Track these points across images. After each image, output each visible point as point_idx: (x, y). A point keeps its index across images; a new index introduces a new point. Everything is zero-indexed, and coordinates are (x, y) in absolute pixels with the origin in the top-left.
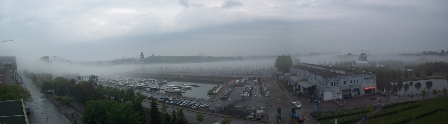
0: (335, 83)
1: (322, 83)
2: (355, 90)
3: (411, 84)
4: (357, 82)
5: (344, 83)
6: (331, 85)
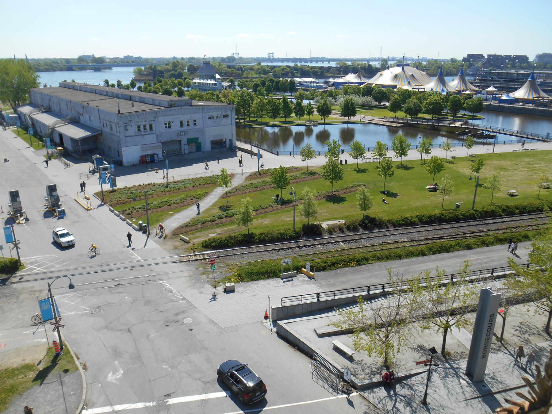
0: (145, 126)
2: (190, 141)
3: (309, 131)
4: (195, 124)
5: (166, 127)
6: (136, 132)
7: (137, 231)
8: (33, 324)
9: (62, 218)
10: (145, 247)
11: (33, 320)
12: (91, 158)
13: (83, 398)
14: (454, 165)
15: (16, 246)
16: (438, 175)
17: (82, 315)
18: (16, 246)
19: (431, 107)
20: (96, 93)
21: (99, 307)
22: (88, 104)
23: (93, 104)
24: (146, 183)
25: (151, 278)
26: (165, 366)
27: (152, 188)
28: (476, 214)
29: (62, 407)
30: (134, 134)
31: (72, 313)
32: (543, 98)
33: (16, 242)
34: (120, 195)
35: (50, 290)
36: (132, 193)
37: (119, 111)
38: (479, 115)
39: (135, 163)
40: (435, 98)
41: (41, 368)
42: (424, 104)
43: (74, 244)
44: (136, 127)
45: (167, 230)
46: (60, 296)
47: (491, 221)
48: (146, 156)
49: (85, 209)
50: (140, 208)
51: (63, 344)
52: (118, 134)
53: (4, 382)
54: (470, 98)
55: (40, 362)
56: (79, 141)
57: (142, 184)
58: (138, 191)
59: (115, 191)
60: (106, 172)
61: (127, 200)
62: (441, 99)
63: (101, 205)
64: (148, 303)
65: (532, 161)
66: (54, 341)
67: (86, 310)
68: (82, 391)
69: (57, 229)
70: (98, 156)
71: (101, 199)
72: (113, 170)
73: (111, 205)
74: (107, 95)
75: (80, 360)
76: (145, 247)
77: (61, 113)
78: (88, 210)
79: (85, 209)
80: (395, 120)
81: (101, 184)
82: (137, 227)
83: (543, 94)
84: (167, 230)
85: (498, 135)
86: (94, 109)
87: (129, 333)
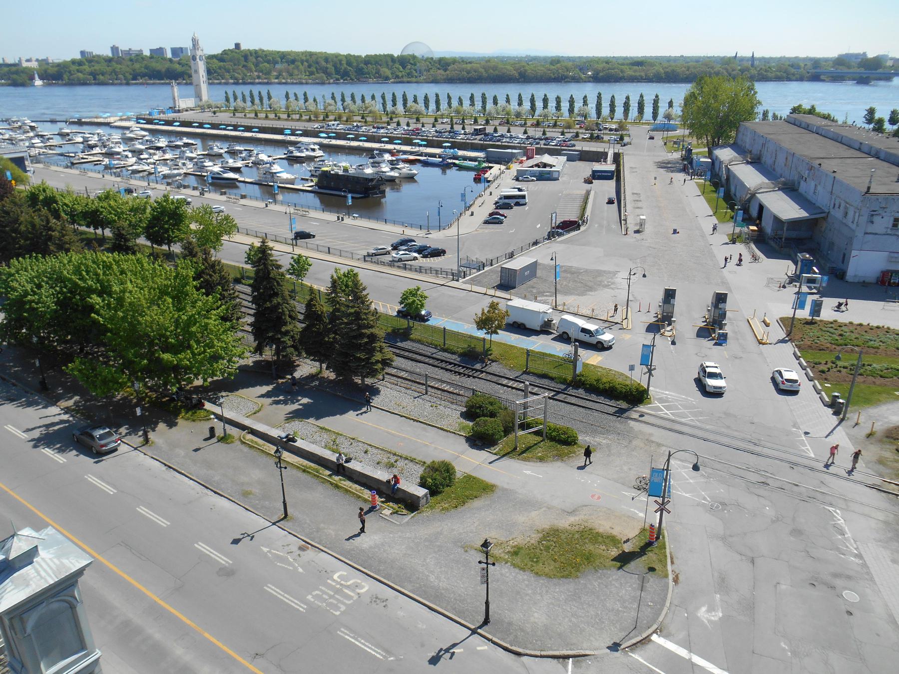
1: (855, 212)
6: (887, 228)
7: (825, 406)
8: (636, 487)
9: (720, 345)
10: (826, 437)
11: (638, 481)
12: (796, 255)
13: (661, 619)
15: (650, 371)
17: (699, 504)
18: (650, 371)
20: (841, 142)
21: (723, 504)
22: (820, 164)
23: (828, 166)
24: (874, 324)
25: (819, 496)
26: (785, 644)
27: (881, 335)
29: (634, 614)
30: (883, 231)
31: (687, 495)
33: (651, 367)
34: (819, 334)
35: (668, 460)
36: (841, 335)
37: (869, 188)
39: (867, 280)
41: (627, 548)
43: (723, 393)
44: (892, 219)
45: (879, 424)
46: (679, 463)
48: (892, 272)
49: (758, 340)
50: (844, 368)
51: (662, 532)
52: (854, 226)
53: (585, 543)
55: (628, 540)
56: (786, 225)
57: (865, 323)
58: (853, 336)
59: (815, 323)
60: (812, 285)
61: (829, 345)
63: (783, 341)
64: (797, 532)
66: (651, 525)
67: (705, 499)
68: (661, 609)
69: (708, 364)
70: (808, 256)
71: (787, 330)
72: (824, 285)
73: (799, 347)
74: (859, 150)
75: (675, 566)
76: (826, 437)
77: (774, 170)
78: (760, 343)
79: (758, 340)
81: (795, 309)
82: (827, 400)
84: (879, 424)
86: (827, 175)
87: (751, 565)
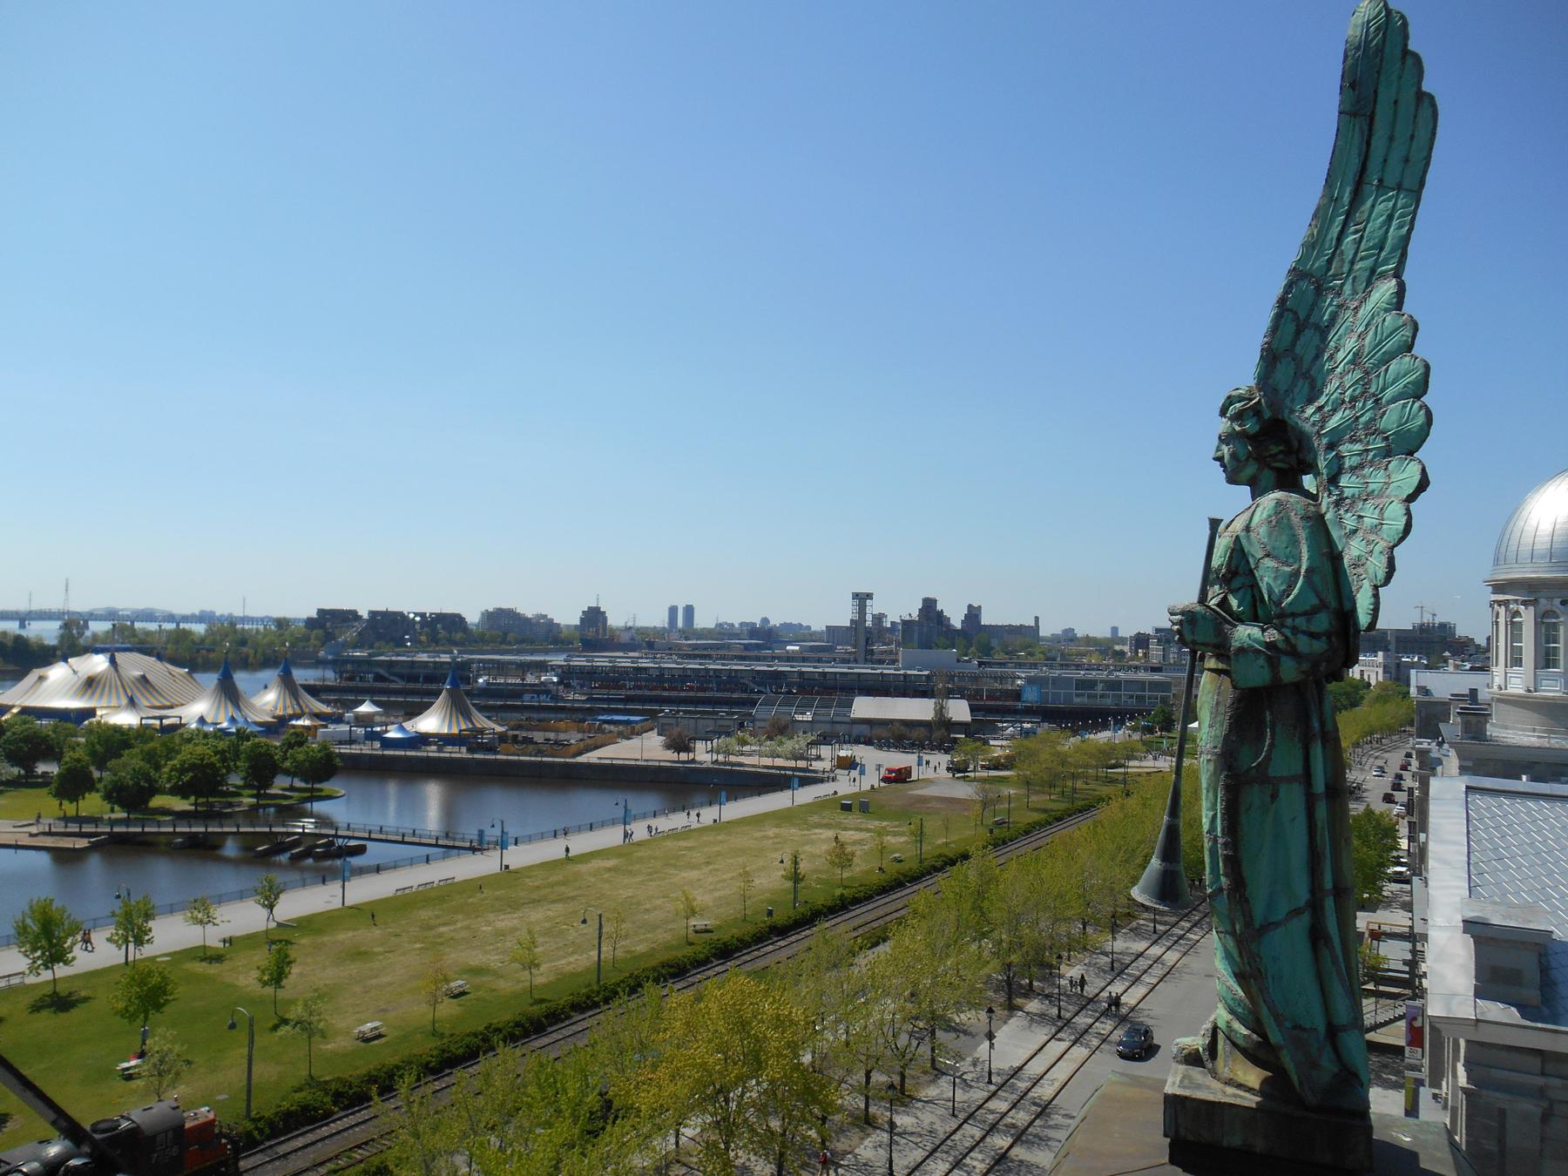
14: (226, 965)
16: (154, 1016)
19: (187, 777)
28: (257, 1128)
32: (481, 731)
38: (327, 787)
40: (200, 750)
42: (166, 770)
47: (300, 1142)
54: (301, 744)
62: (216, 753)
65: (437, 917)
80: (74, 828)
83: (482, 721)
85: (369, 844)
